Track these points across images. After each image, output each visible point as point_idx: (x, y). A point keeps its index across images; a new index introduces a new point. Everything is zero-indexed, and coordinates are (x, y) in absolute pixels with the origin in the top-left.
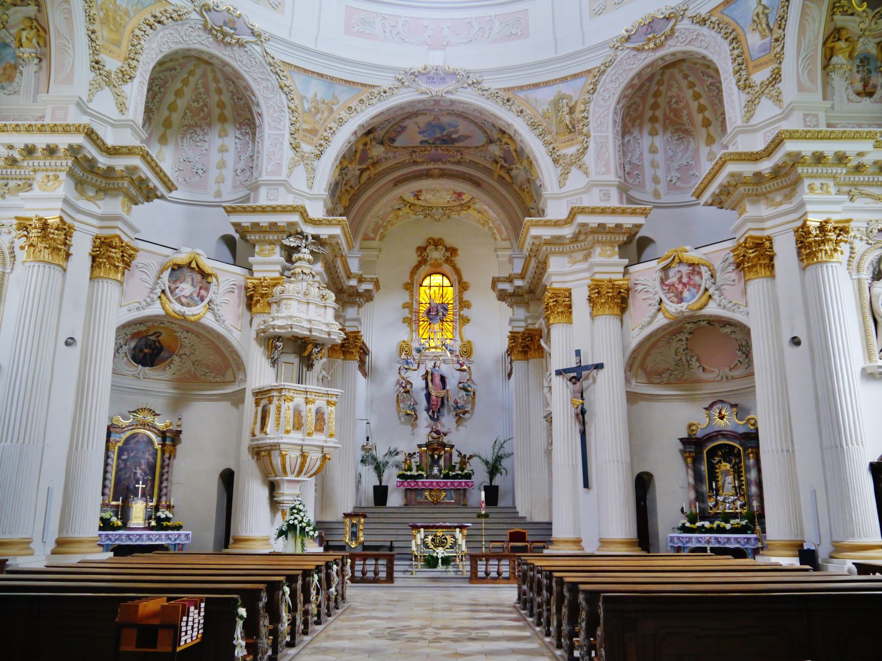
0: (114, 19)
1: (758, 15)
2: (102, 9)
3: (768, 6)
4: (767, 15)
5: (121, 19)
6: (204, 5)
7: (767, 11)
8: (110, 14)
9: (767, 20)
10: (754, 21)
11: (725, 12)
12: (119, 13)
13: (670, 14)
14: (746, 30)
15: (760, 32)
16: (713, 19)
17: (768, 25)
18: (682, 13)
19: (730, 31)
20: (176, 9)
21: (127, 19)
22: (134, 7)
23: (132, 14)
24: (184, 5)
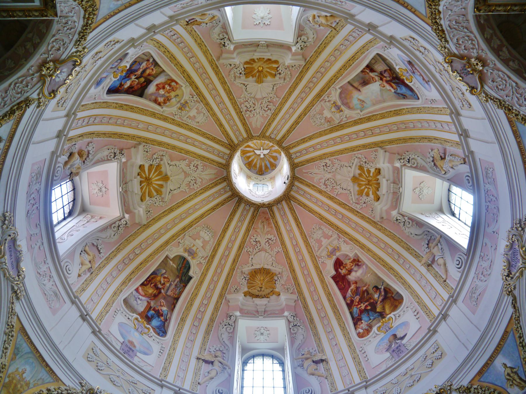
0: (16, 385)
1: (508, 375)
2: (9, 377)
3: (513, 367)
4: (516, 373)
5: (21, 387)
6: (90, 389)
7: (515, 370)
8: (14, 381)
9: (518, 376)
10: (508, 379)
11: (481, 380)
12: (22, 382)
13: (440, 390)
14: (505, 387)
15: (517, 386)
16: (476, 387)
17: (521, 379)
18: (449, 388)
19: (492, 390)
20: (68, 388)
21: (26, 388)
22: (36, 382)
23: (31, 386)
24: (75, 387)
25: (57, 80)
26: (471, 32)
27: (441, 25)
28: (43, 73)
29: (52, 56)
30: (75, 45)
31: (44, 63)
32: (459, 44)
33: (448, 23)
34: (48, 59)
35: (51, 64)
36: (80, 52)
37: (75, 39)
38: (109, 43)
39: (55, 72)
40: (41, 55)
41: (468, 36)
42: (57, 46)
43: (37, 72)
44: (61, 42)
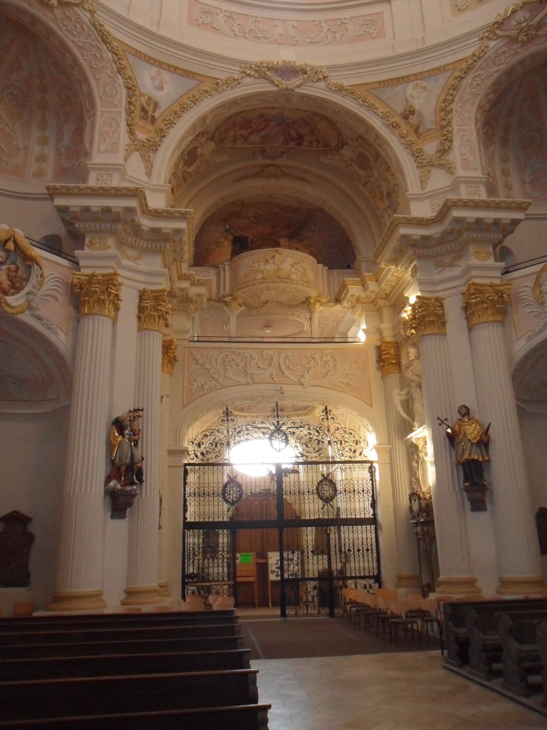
25: (528, 15)
26: (74, 42)
27: (109, 50)
28: (534, 32)
29: (514, 47)
30: (485, 53)
31: (524, 43)
32: (78, 22)
33: (104, 55)
34: (520, 45)
35: (520, 39)
36: (487, 37)
37: (482, 60)
38: (462, 8)
39: (522, 29)
40: (522, 53)
41: (74, 36)
42: (502, 57)
43: (539, 35)
44: (496, 61)
